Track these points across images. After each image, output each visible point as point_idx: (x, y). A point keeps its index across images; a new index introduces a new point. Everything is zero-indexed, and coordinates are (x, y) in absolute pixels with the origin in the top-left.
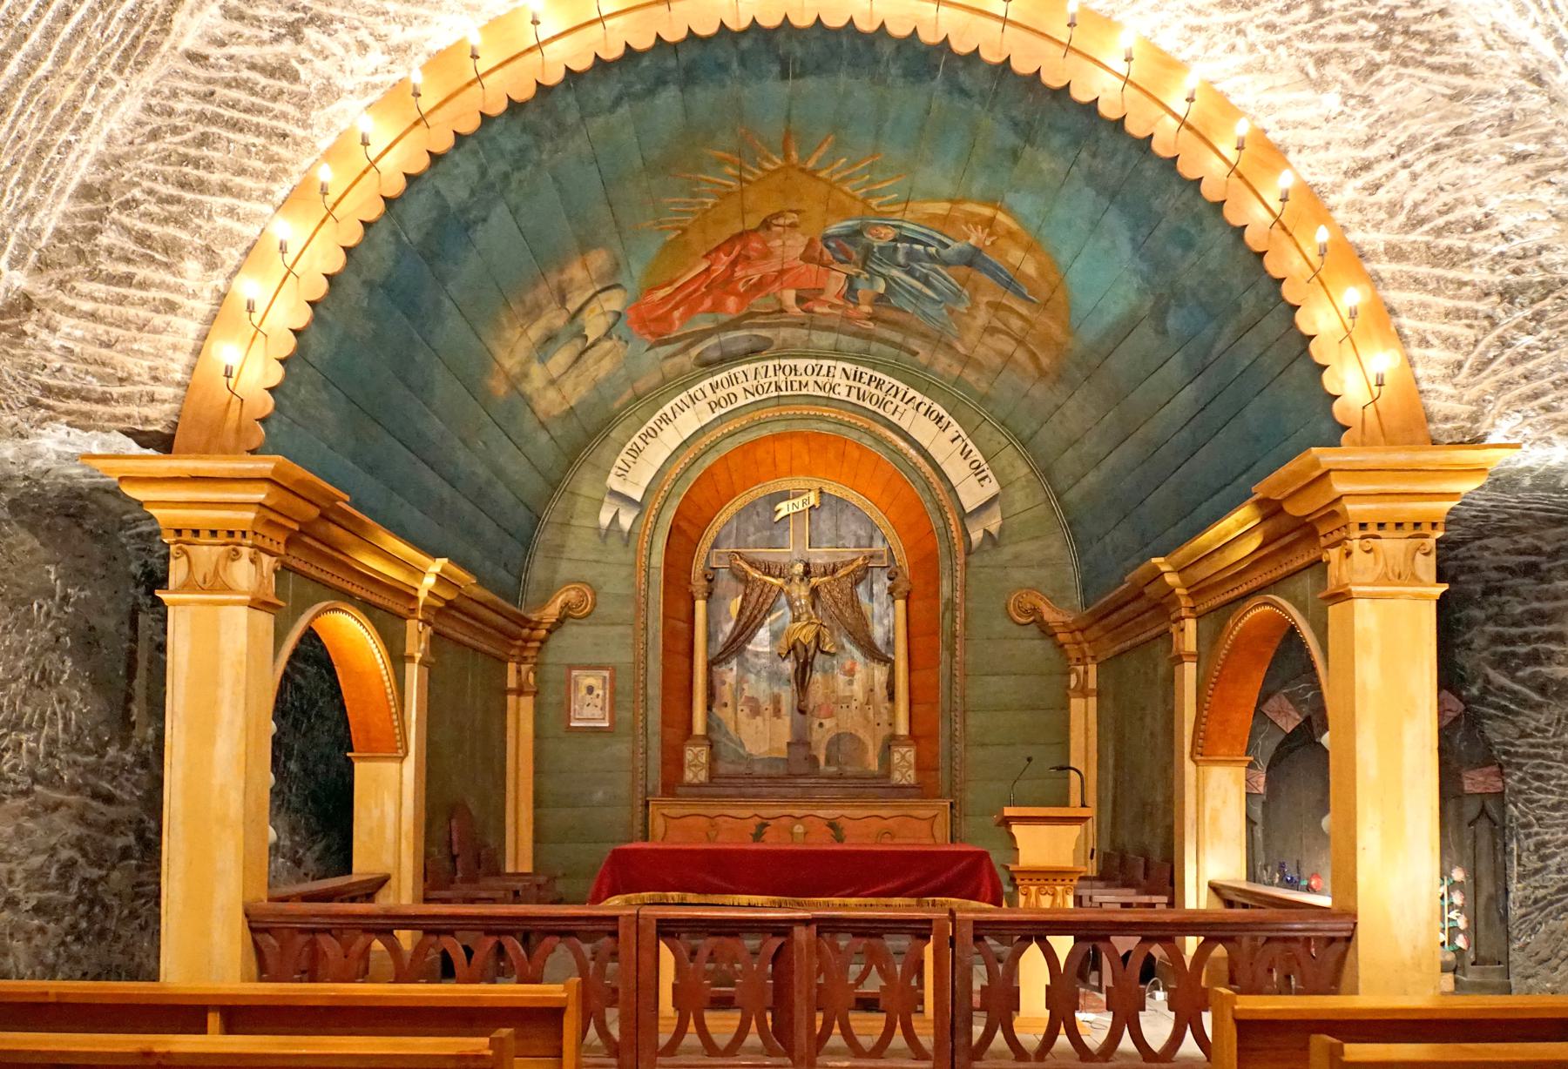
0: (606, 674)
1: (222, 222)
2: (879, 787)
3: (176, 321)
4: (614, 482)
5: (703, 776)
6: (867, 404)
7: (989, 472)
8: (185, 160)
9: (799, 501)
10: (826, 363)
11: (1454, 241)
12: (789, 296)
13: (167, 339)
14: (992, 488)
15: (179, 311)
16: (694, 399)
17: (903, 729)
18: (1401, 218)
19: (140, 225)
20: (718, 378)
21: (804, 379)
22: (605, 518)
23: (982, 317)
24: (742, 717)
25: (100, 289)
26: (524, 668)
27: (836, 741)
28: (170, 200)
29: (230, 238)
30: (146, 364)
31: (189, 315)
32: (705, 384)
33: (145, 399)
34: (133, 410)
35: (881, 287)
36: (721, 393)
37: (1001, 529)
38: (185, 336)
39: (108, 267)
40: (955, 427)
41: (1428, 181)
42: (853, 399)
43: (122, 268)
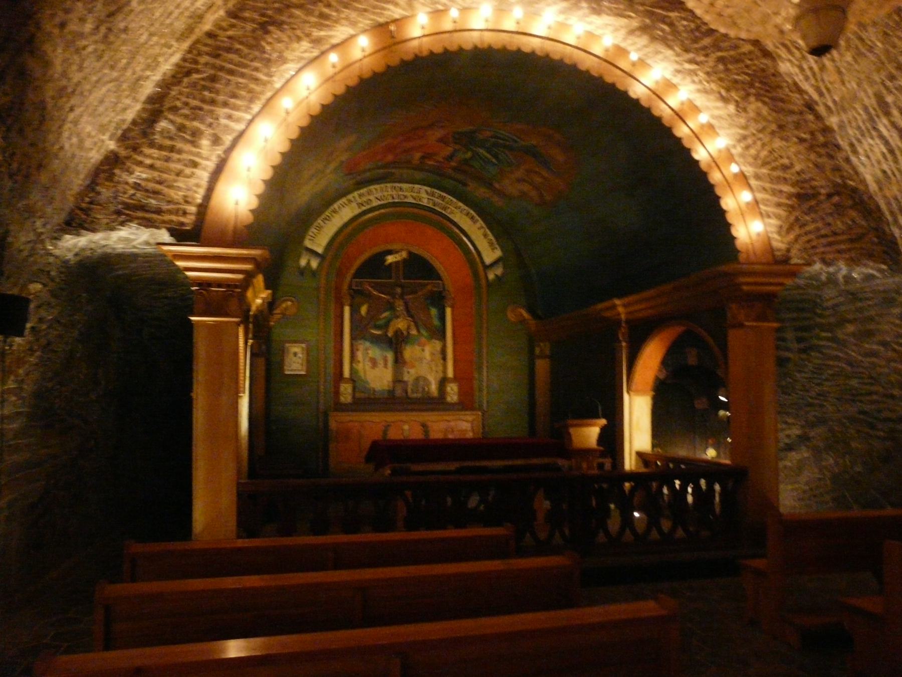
0: (304, 345)
1: (223, 121)
2: (437, 403)
3: (198, 172)
4: (308, 243)
6: (437, 208)
7: (497, 246)
9: (397, 255)
10: (417, 186)
12: (418, 155)
13: (193, 181)
14: (498, 253)
15: (199, 167)
16: (350, 201)
17: (450, 373)
19: (179, 120)
20: (362, 191)
21: (405, 194)
22: (303, 262)
23: (519, 173)
24: (367, 368)
25: (155, 152)
27: (417, 379)
30: (181, 193)
31: (204, 169)
32: (356, 194)
33: (181, 212)
34: (174, 218)
35: (469, 154)
36: (365, 199)
37: (503, 274)
38: (202, 179)
40: (481, 222)
42: (431, 205)
43: (168, 143)
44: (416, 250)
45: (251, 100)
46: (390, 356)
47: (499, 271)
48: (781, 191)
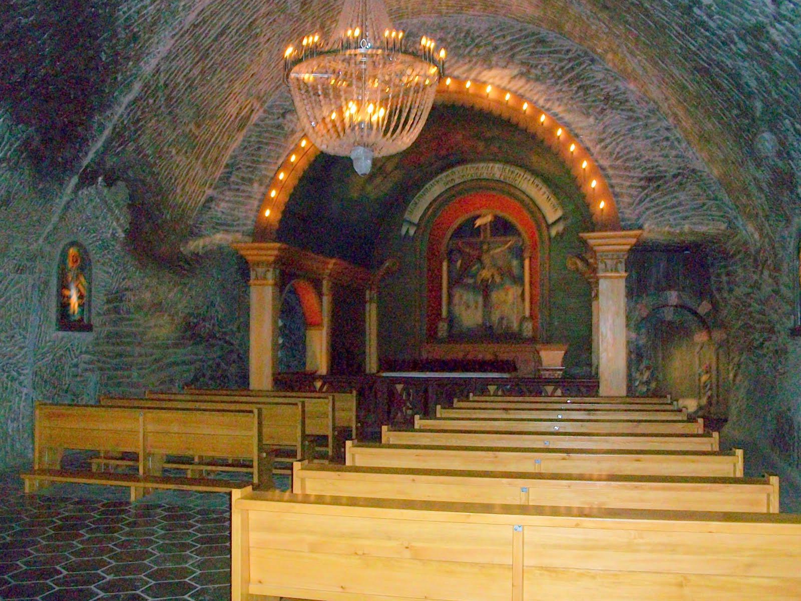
3: (251, 201)
5: (445, 334)
8: (253, 155)
11: (631, 164)
14: (559, 213)
17: (527, 313)
18: (614, 156)
25: (231, 193)
26: (373, 292)
28: (249, 167)
29: (266, 176)
39: (233, 187)
41: (622, 145)
43: (237, 187)
44: (501, 214)
45: (278, 158)
46: (480, 300)
47: (560, 227)
48: (633, 177)
